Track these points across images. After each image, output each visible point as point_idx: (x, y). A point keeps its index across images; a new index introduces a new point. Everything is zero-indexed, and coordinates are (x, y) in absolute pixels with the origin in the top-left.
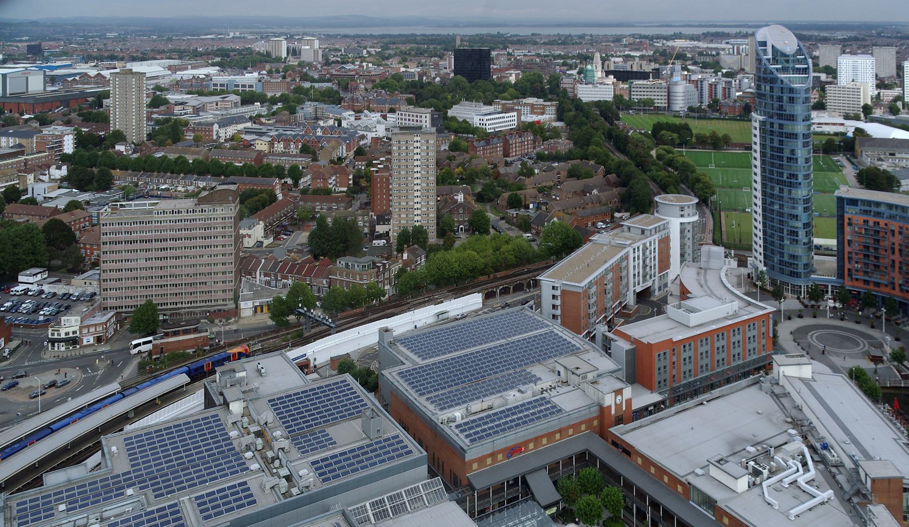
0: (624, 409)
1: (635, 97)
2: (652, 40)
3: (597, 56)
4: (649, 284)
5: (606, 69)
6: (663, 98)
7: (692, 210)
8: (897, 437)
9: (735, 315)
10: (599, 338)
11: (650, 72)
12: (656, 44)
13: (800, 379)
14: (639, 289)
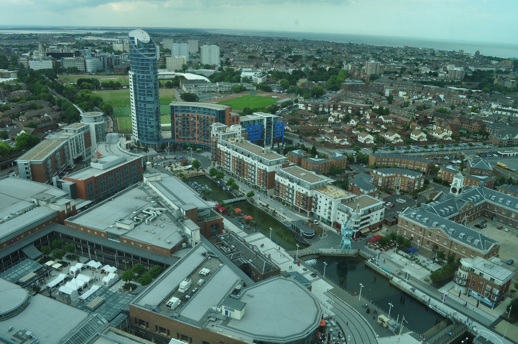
0: (72, 210)
1: (66, 66)
2: (74, 37)
3: (40, 46)
4: (81, 154)
5: (47, 52)
6: (82, 66)
7: (101, 118)
8: (195, 194)
9: (125, 161)
10: (55, 183)
11: (73, 53)
12: (76, 39)
13: (156, 181)
14: (75, 158)
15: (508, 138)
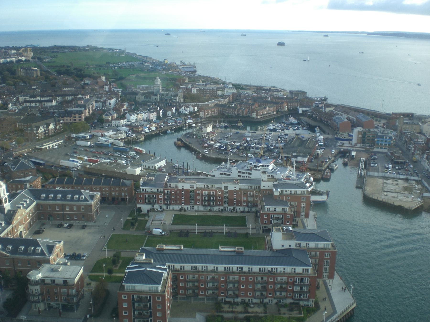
15: (43, 130)
